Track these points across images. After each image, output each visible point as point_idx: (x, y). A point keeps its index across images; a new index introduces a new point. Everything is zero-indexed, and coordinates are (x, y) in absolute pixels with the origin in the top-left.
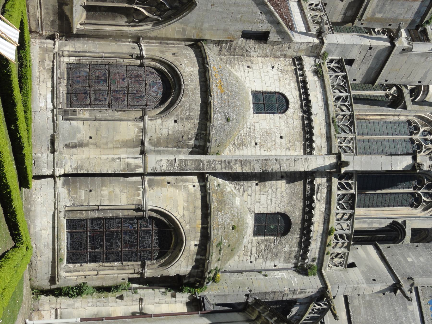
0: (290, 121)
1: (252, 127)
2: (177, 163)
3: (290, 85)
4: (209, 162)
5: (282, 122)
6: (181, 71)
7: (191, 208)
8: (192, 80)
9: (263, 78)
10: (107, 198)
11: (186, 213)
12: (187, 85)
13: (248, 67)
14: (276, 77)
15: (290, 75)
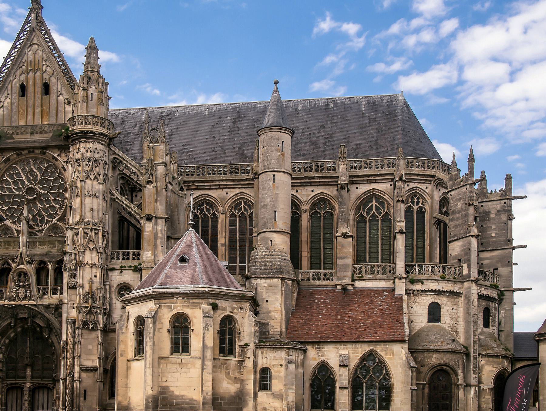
0: (445, 302)
1: (448, 325)
2: (474, 369)
3: (424, 300)
4: (474, 352)
5: (445, 307)
6: (435, 364)
7: (492, 364)
8: (441, 359)
9: (420, 315)
10: (487, 405)
11: (495, 366)
12: (444, 361)
13: (412, 322)
14: (419, 307)
15: (417, 298)
